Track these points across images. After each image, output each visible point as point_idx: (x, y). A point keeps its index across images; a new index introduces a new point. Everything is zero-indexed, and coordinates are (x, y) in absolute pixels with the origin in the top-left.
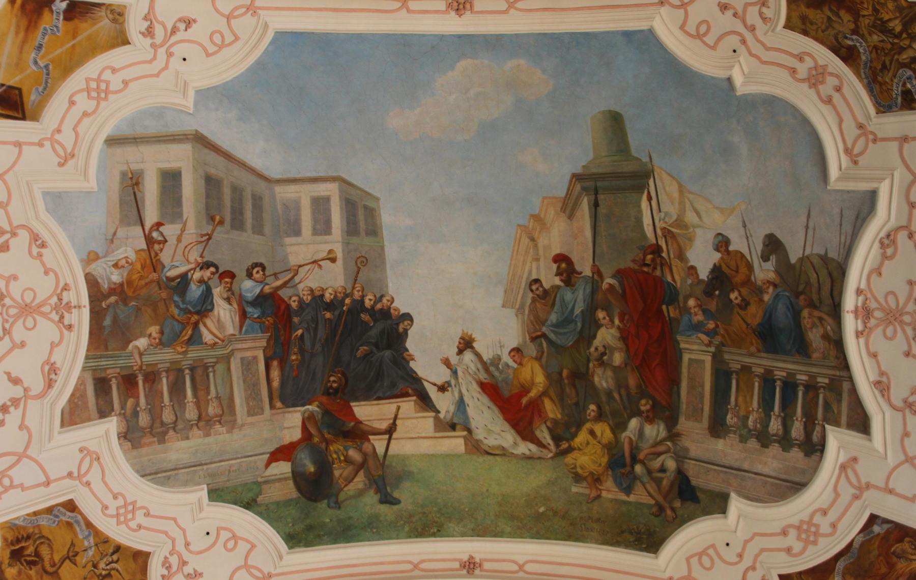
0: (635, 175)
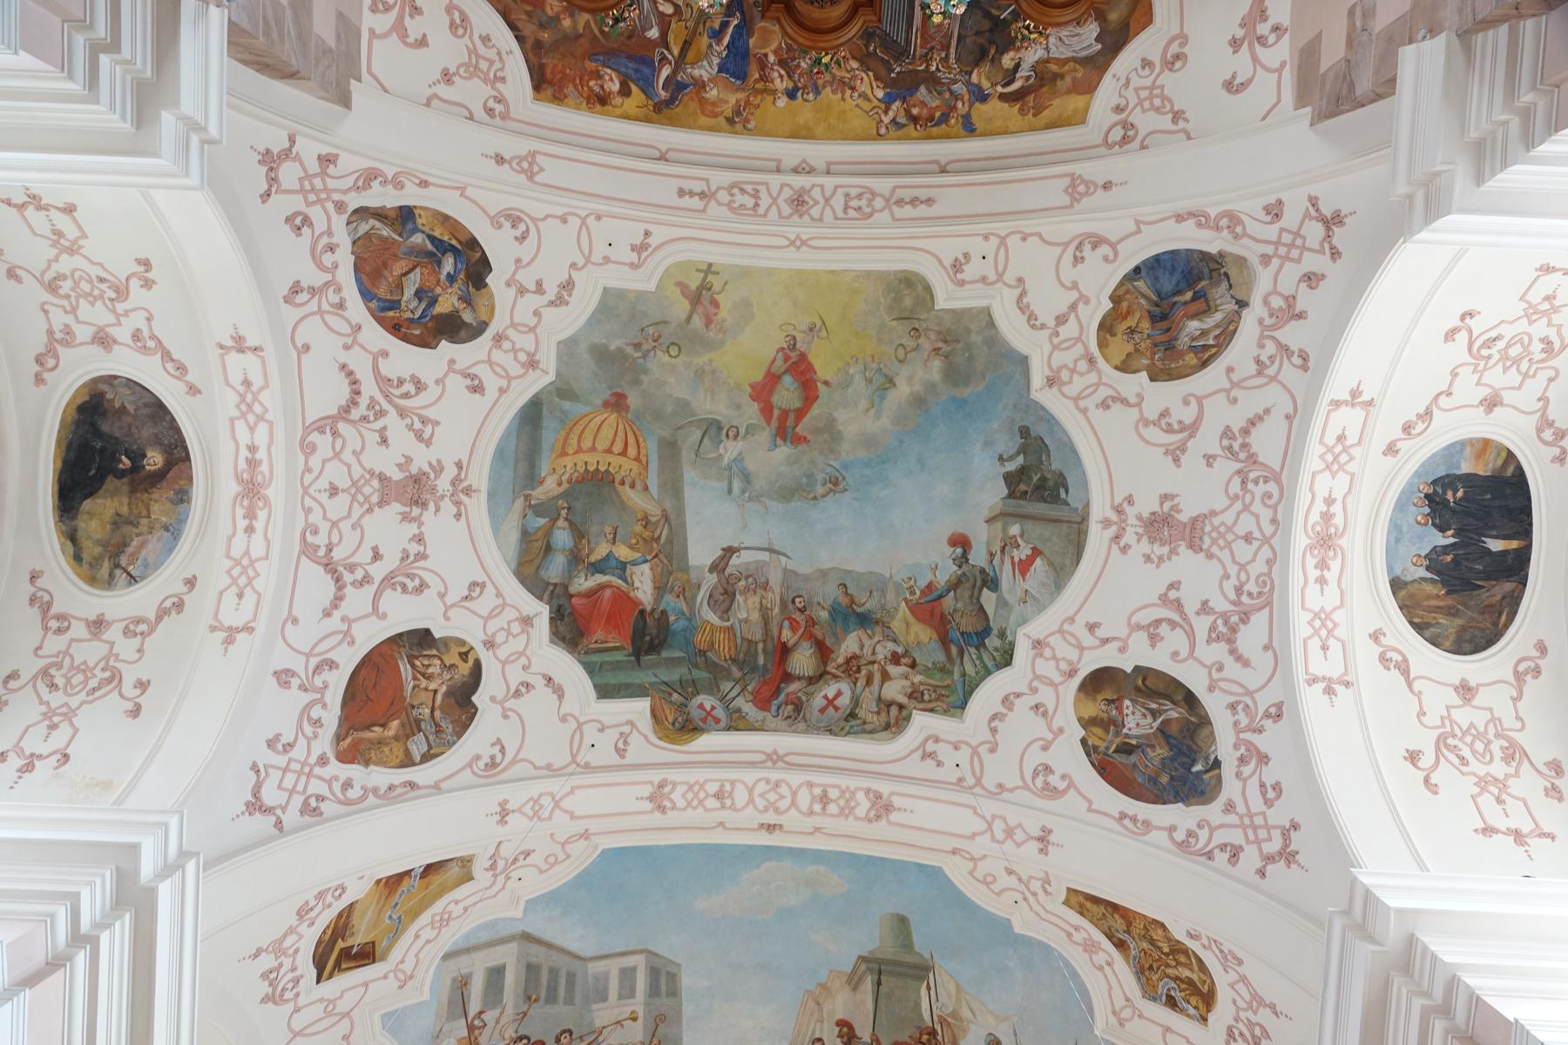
0: (916, 967)
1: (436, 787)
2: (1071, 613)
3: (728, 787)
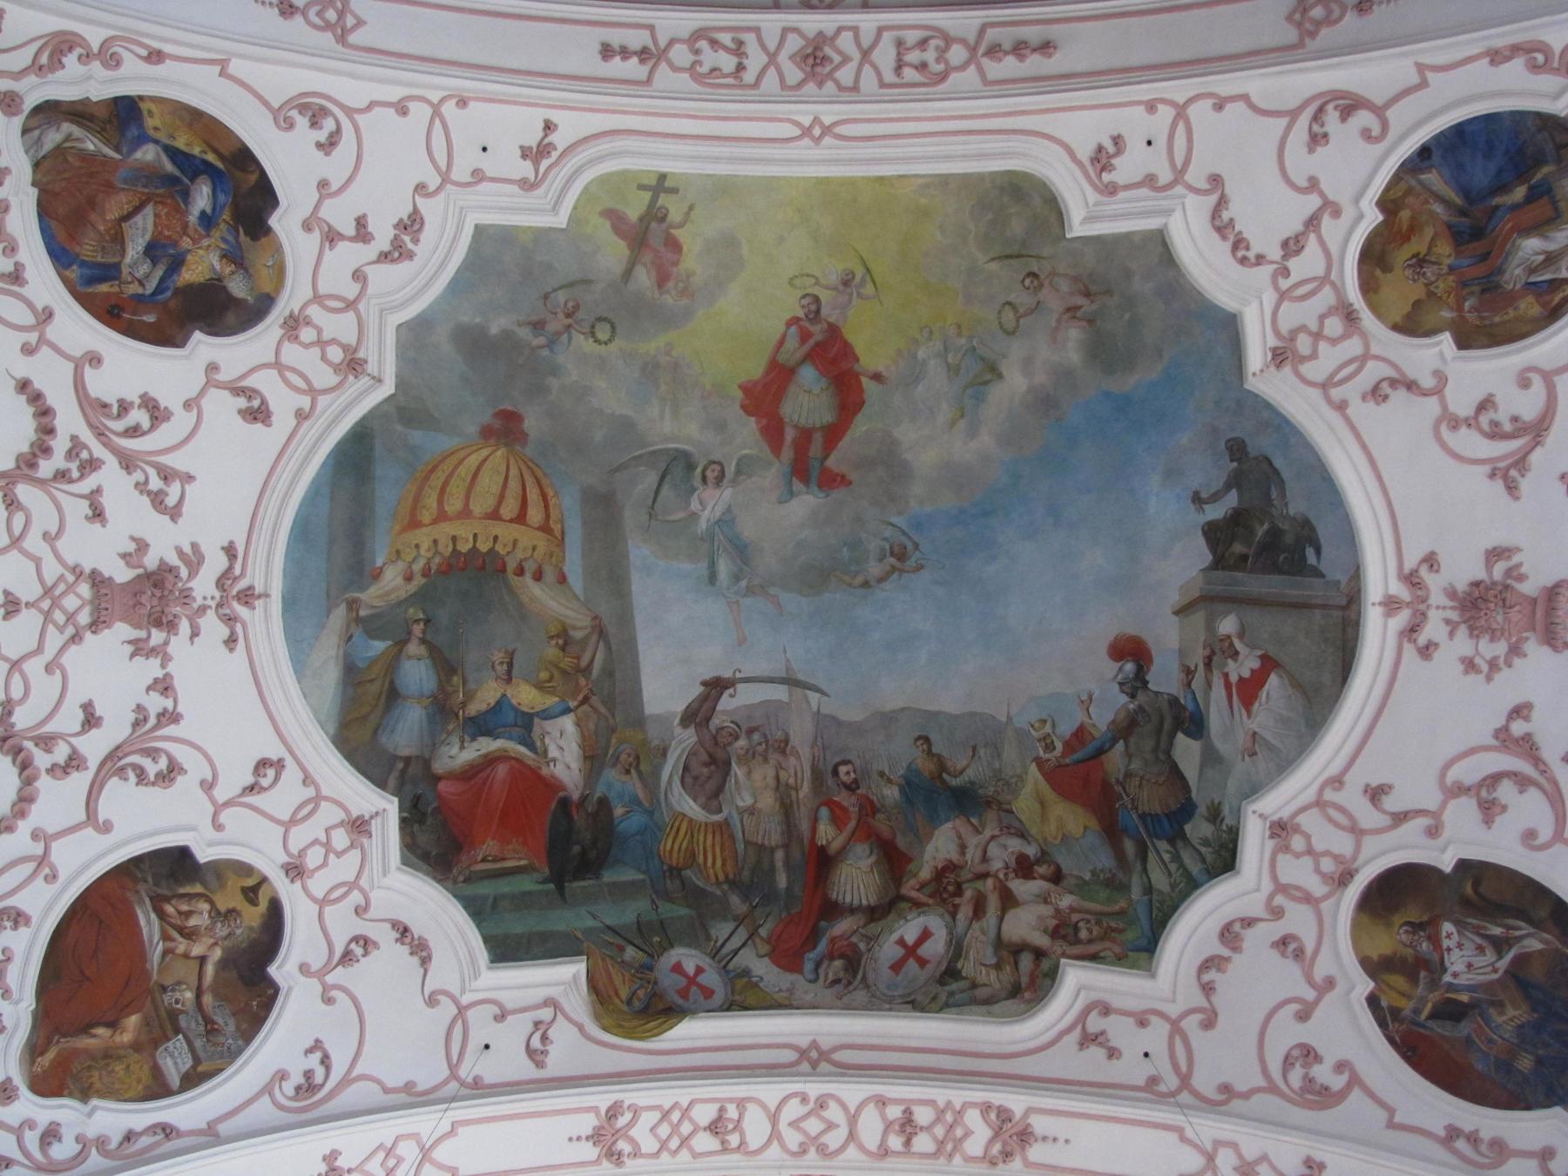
1: (211, 1136)
2: (1334, 769)
3: (732, 1112)
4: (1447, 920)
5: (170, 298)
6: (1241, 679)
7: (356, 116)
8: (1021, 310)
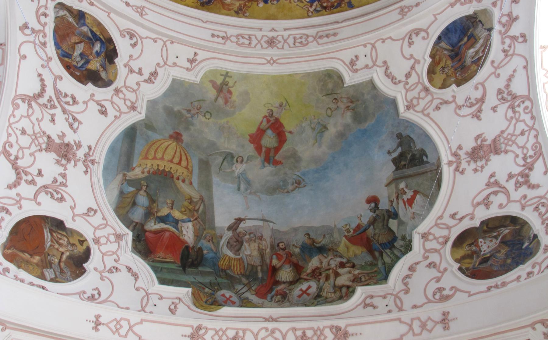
2: (440, 214)
3: (241, 334)
4: (479, 239)
5: (84, 70)
6: (408, 199)
7: (143, 40)
8: (333, 109)
